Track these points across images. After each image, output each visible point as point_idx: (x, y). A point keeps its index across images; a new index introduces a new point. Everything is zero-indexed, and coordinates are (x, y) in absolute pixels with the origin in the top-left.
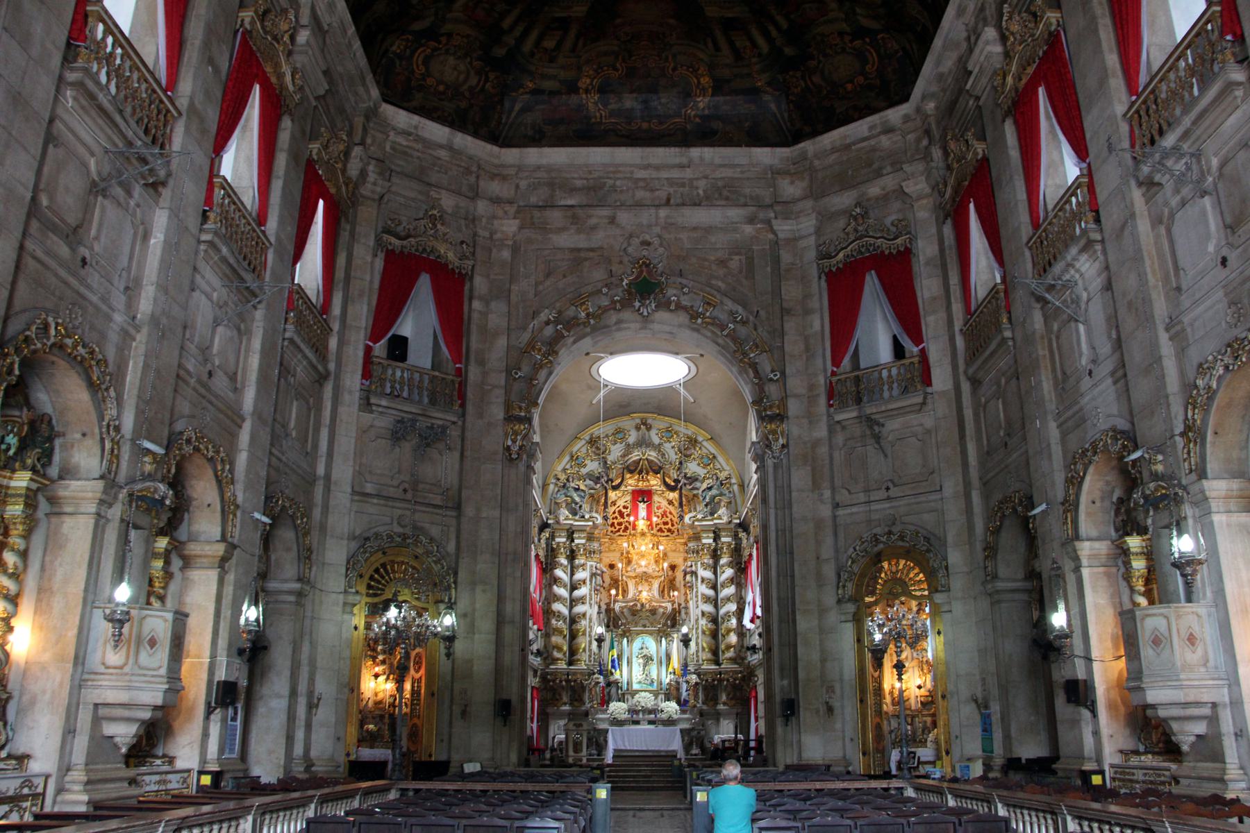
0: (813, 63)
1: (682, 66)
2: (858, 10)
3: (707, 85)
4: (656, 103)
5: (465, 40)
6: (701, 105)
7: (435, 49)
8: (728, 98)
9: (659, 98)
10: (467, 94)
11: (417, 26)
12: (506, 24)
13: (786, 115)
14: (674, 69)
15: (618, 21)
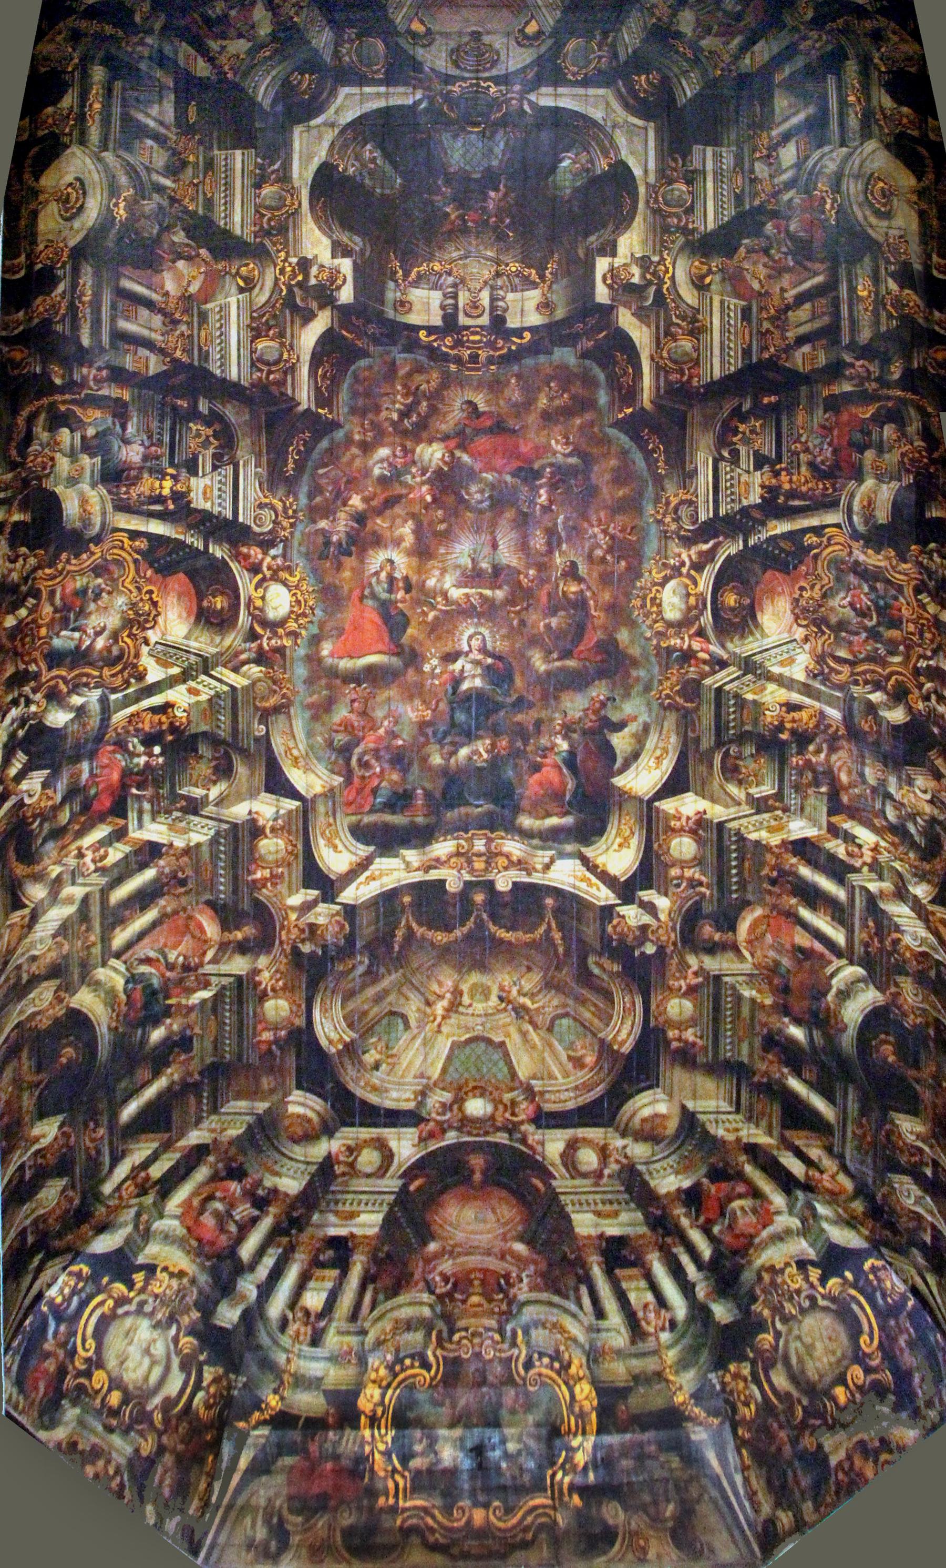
0: (766, 1339)
1: (541, 1355)
2: (821, 1209)
3: (587, 1405)
4: (497, 1453)
5: (175, 1283)
6: (580, 1458)
7: (121, 1301)
8: (628, 1436)
9: (503, 1441)
10: (158, 1417)
11: (104, 1244)
12: (246, 1251)
13: (738, 1479)
14: (528, 1365)
15: (433, 1247)
